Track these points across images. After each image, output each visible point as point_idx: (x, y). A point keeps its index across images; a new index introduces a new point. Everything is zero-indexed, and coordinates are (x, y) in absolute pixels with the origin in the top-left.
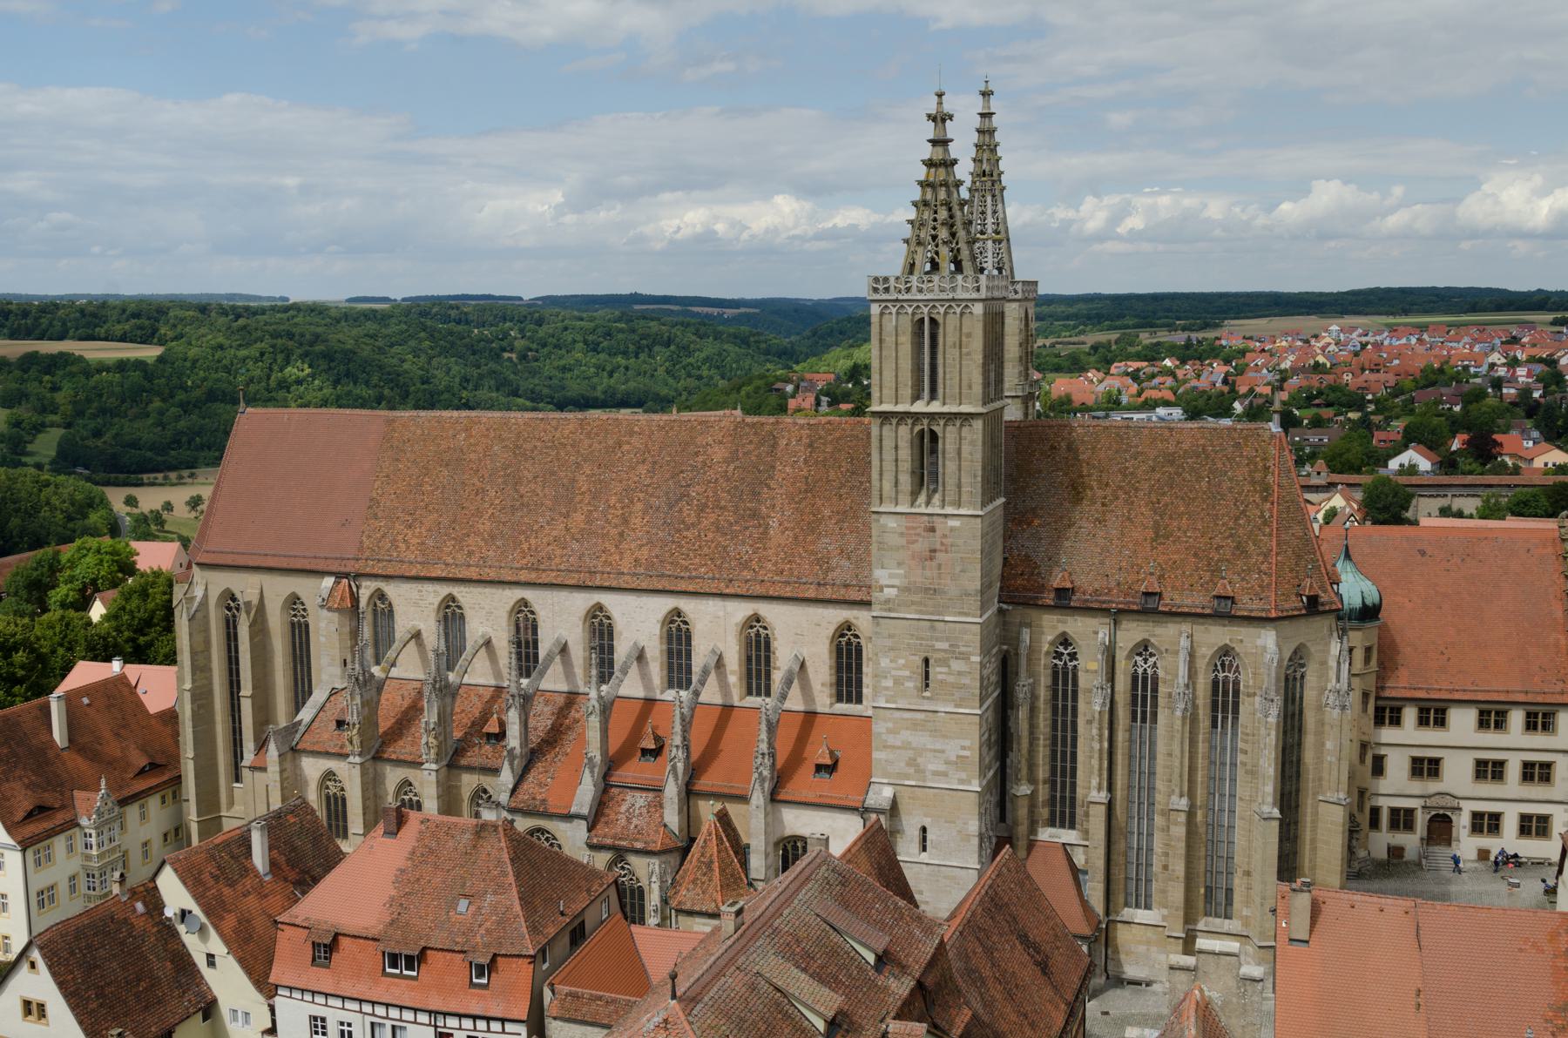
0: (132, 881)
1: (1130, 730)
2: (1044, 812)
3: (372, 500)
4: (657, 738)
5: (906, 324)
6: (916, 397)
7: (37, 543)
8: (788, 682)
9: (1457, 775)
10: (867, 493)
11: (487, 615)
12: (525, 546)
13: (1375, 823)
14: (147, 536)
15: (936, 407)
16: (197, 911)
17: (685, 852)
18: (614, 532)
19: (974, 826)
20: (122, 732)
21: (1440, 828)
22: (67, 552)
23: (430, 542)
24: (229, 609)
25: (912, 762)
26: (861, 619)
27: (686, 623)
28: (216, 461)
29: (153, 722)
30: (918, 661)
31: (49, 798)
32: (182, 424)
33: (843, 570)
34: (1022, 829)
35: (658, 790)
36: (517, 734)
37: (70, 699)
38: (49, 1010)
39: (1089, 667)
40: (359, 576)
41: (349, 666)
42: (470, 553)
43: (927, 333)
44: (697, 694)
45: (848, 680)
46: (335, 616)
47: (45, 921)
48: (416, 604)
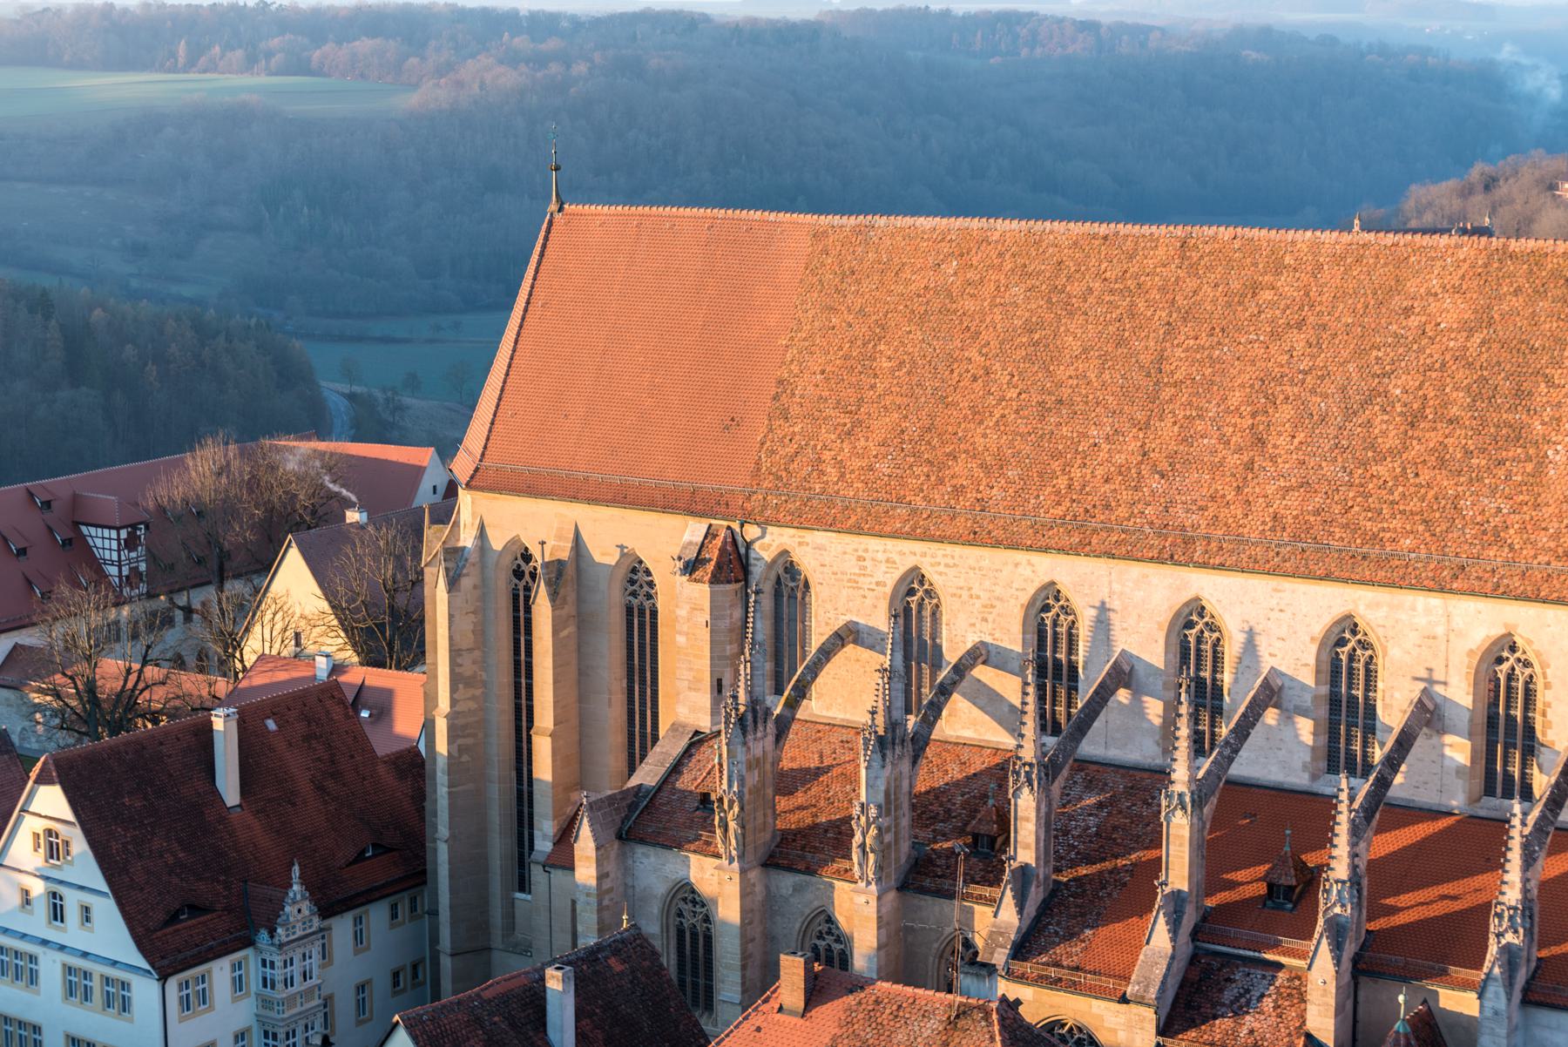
3: (780, 382)
4: (1301, 867)
12: (1062, 482)
18: (1233, 460)
20: (330, 784)
23: (883, 467)
24: (518, 574)
27: (1365, 645)
29: (381, 769)
36: (1032, 840)
41: (727, 693)
42: (958, 491)
44: (1383, 783)
48: (854, 584)
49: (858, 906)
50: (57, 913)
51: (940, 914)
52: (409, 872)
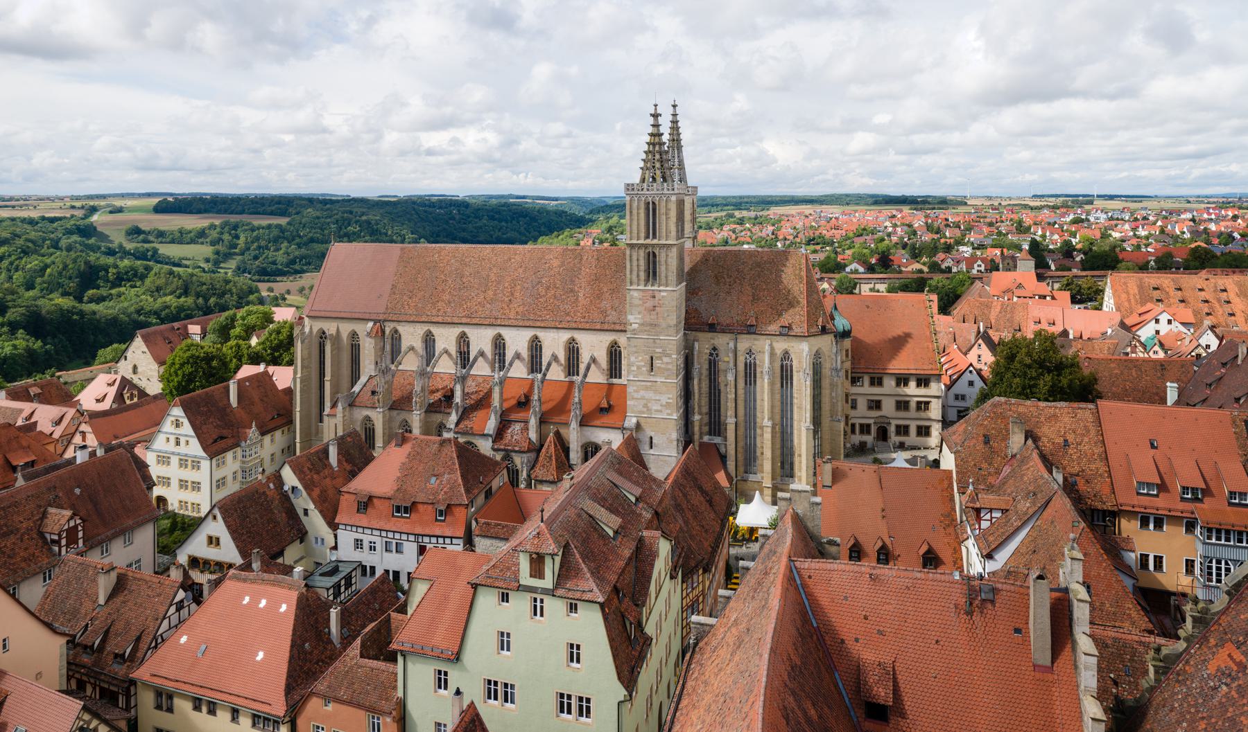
0: (267, 473)
1: (745, 389)
2: (706, 429)
5: (642, 206)
6: (647, 237)
7: (224, 308)
8: (588, 368)
9: (888, 407)
10: (624, 281)
11: (446, 339)
13: (853, 432)
14: (278, 305)
15: (655, 241)
16: (300, 487)
17: (539, 451)
19: (674, 435)
21: (883, 434)
22: (241, 313)
25: (645, 406)
26: (622, 340)
28: (318, 268)
30: (648, 358)
31: (225, 432)
32: (297, 253)
33: (612, 316)
34: (696, 437)
35: (526, 422)
37: (240, 383)
38: (221, 541)
39: (726, 359)
40: (385, 321)
43: (651, 210)
44: (545, 375)
45: (615, 367)
46: (373, 341)
47: (221, 495)
49: (416, 419)
50: (178, 443)
51: (438, 418)
52: (290, 422)
